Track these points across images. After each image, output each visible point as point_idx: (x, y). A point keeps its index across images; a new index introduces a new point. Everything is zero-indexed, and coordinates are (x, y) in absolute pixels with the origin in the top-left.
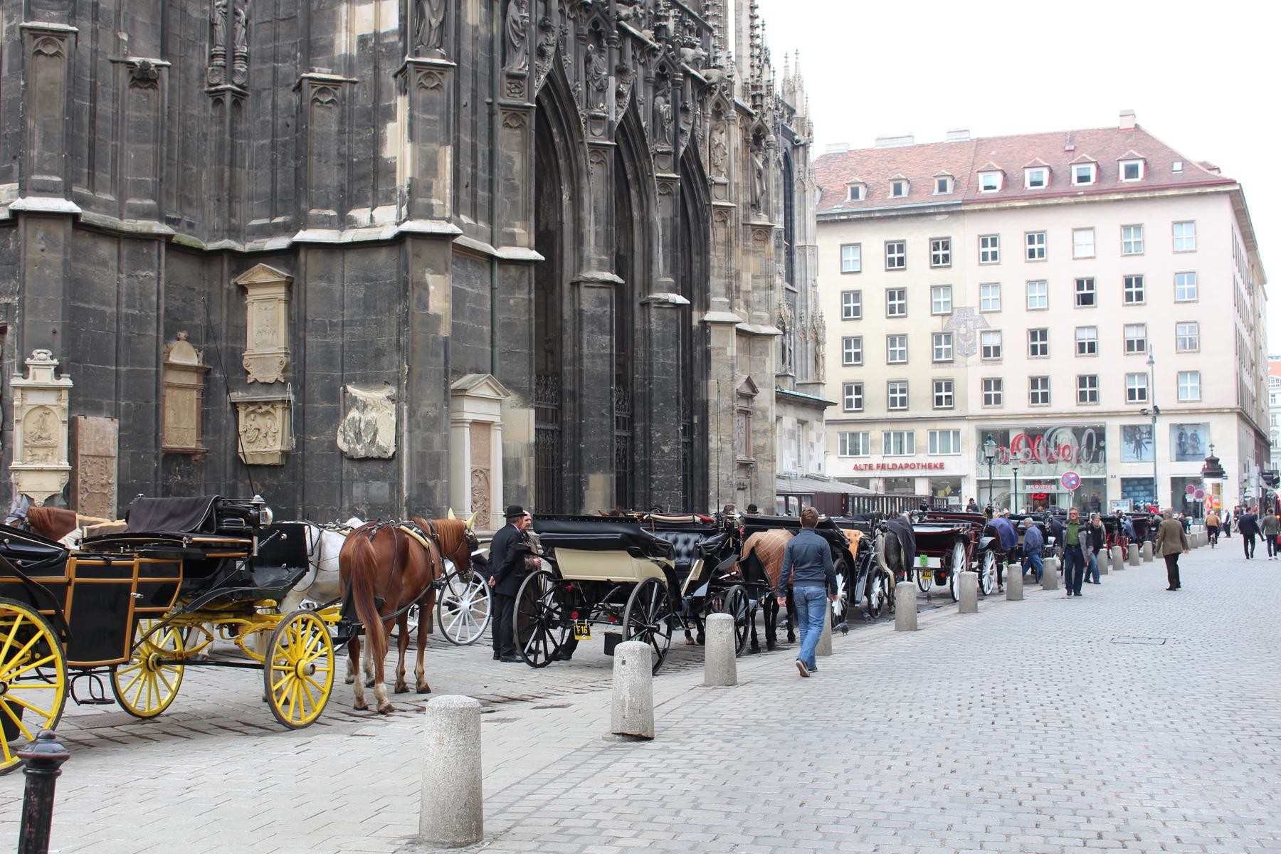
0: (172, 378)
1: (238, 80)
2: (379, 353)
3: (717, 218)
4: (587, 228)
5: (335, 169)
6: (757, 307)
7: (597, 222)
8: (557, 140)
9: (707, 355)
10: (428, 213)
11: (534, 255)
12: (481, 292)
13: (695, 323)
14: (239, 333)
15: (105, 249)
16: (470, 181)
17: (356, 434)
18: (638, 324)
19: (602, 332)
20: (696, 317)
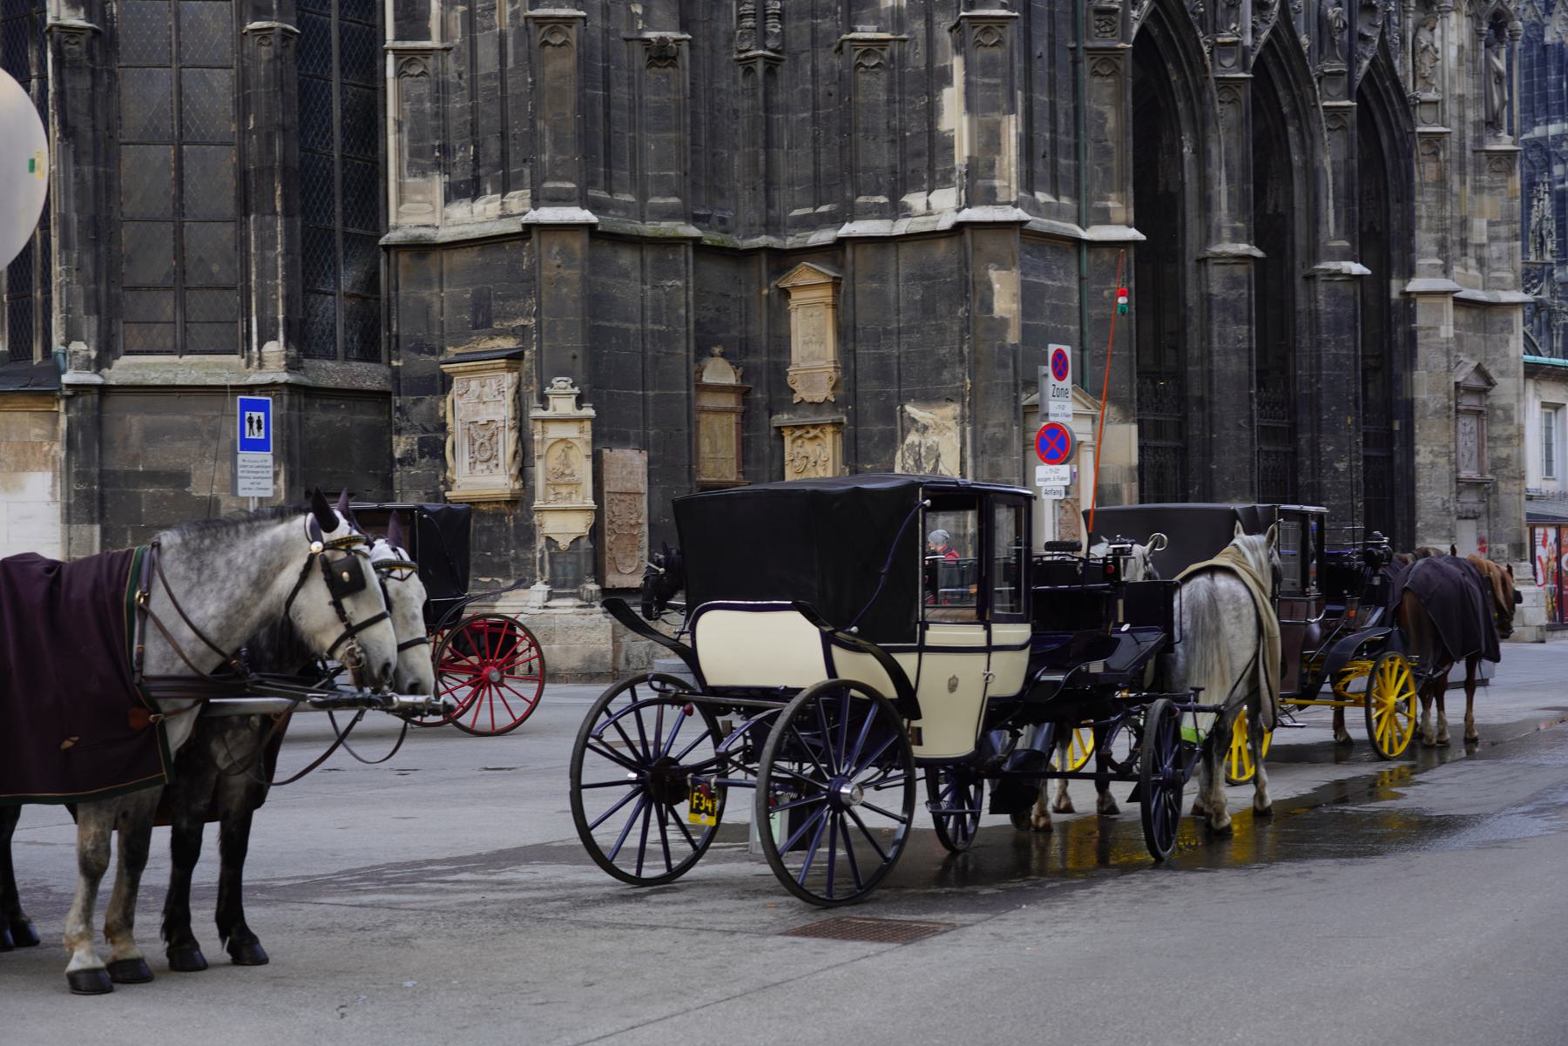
0: (708, 401)
1: (770, 44)
2: (942, 365)
3: (1425, 150)
4: (1216, 188)
5: (886, 146)
6: (1495, 266)
7: (1230, 179)
8: (1174, 78)
9: (1412, 337)
10: (990, 198)
11: (1133, 234)
12: (1065, 284)
13: (1395, 295)
14: (781, 344)
15: (626, 258)
16: (1048, 149)
17: (915, 461)
18: (1301, 304)
19: (1237, 321)
20: (1396, 287)
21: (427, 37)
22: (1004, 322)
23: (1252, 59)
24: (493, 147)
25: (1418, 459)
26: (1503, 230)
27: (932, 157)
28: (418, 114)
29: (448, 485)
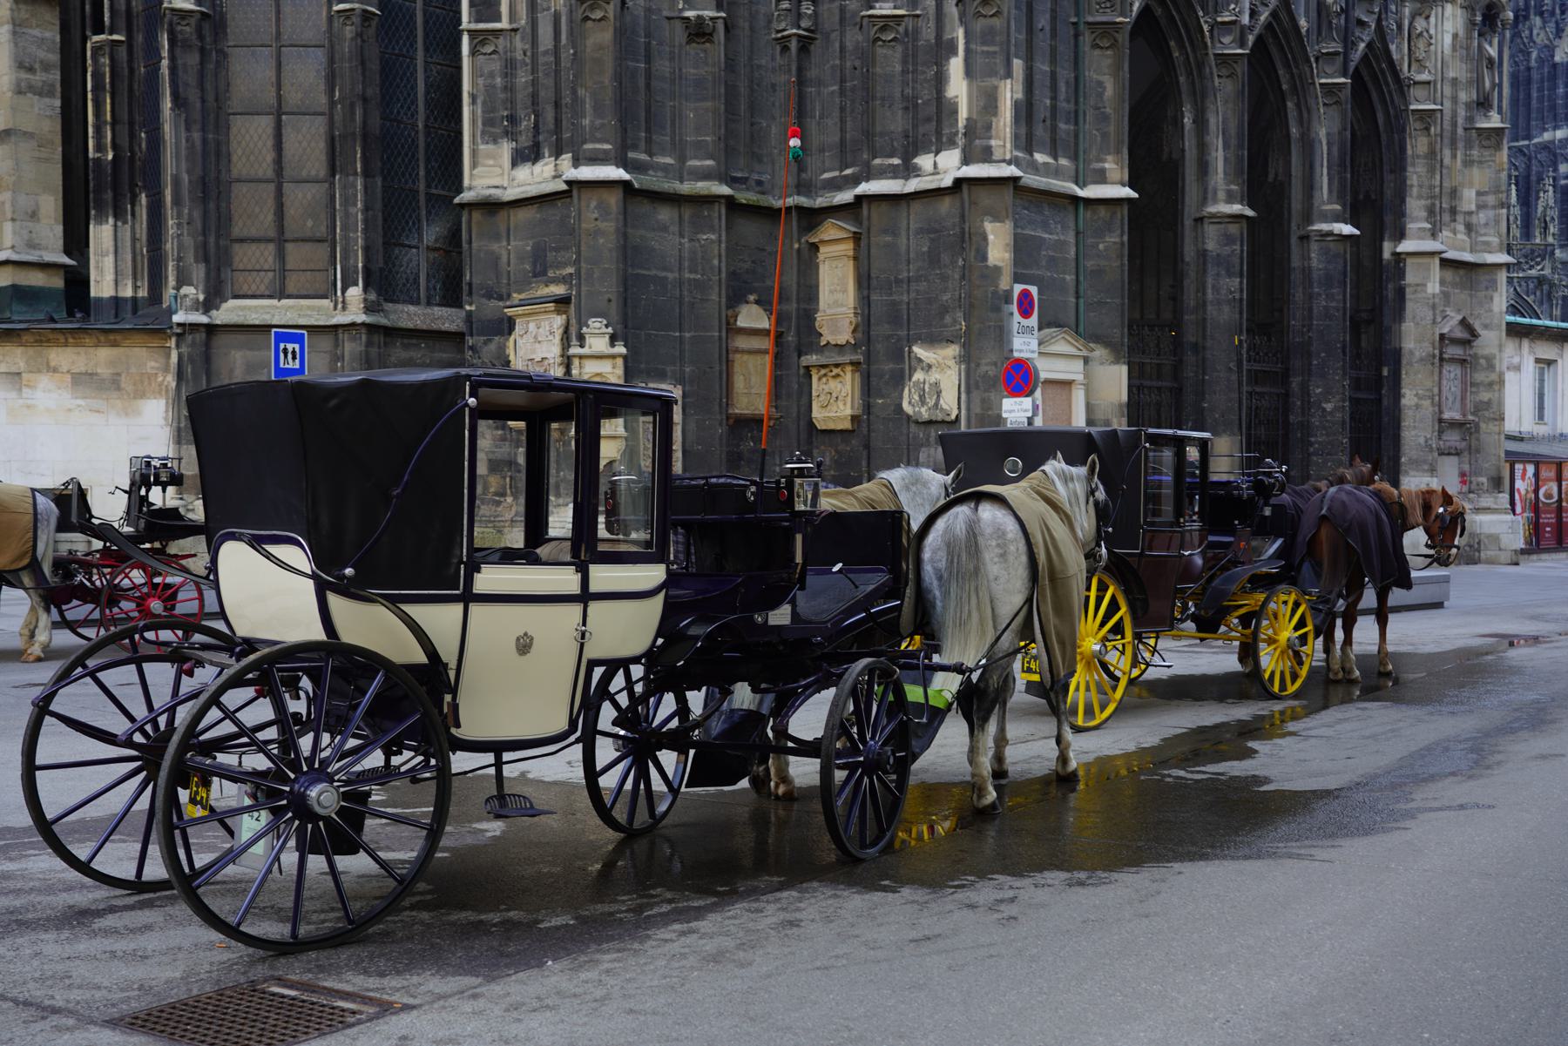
0: (742, 342)
1: (804, 24)
2: (944, 310)
3: (1418, 125)
4: (1214, 154)
5: (900, 112)
7: (1226, 146)
8: (1176, 54)
9: (1401, 293)
10: (986, 156)
11: (1127, 192)
12: (1062, 238)
13: (1386, 255)
14: (809, 294)
15: (665, 214)
16: (1048, 114)
17: (920, 396)
18: (1296, 262)
19: (1230, 275)
20: (1387, 249)
21: (498, 19)
22: (997, 269)
23: (1251, 39)
24: (549, 115)
25: (1404, 401)
26: (1491, 200)
27: (939, 122)
28: (490, 88)
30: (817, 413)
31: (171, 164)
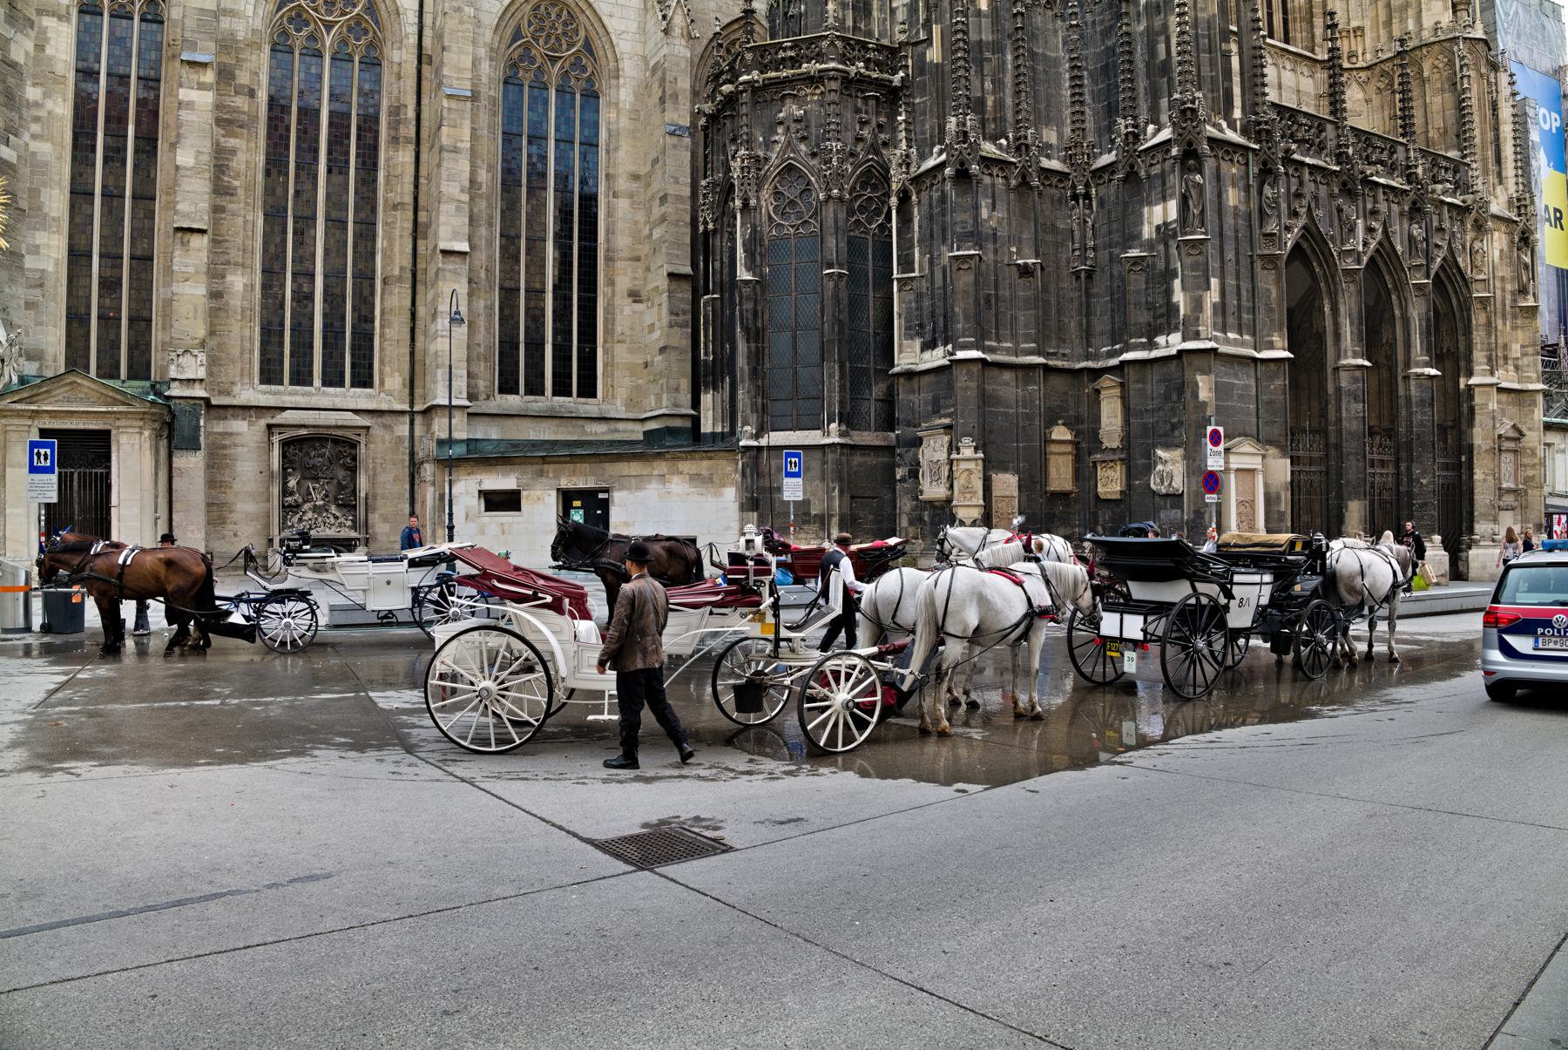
0: (1053, 448)
3: (1479, 306)
7: (1352, 324)
9: (1472, 410)
11: (1287, 354)
13: (1462, 386)
15: (1007, 376)
18: (1401, 392)
20: (1462, 382)
22: (1205, 403)
23: (1365, 259)
25: (1476, 477)
26: (1530, 350)
27: (1169, 317)
28: (909, 309)
29: (922, 492)
30: (1100, 489)
31: (741, 362)
